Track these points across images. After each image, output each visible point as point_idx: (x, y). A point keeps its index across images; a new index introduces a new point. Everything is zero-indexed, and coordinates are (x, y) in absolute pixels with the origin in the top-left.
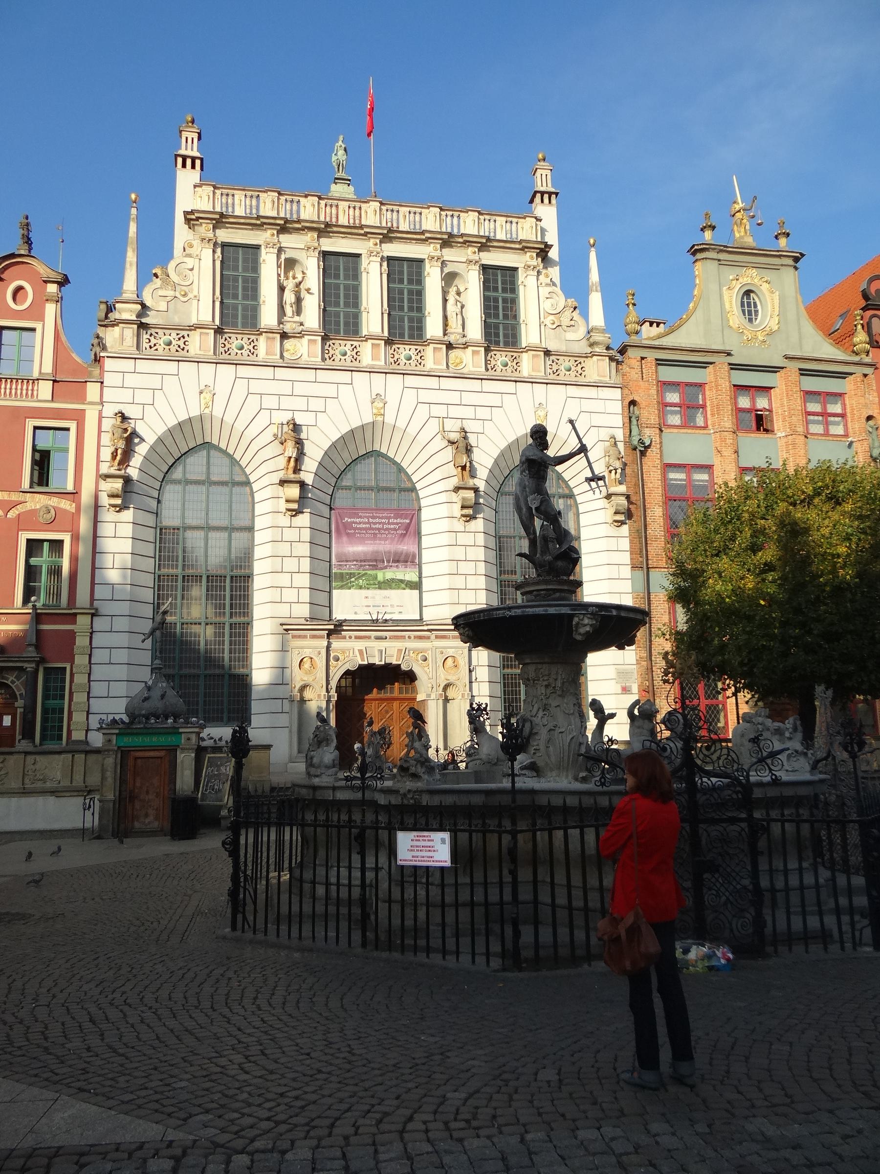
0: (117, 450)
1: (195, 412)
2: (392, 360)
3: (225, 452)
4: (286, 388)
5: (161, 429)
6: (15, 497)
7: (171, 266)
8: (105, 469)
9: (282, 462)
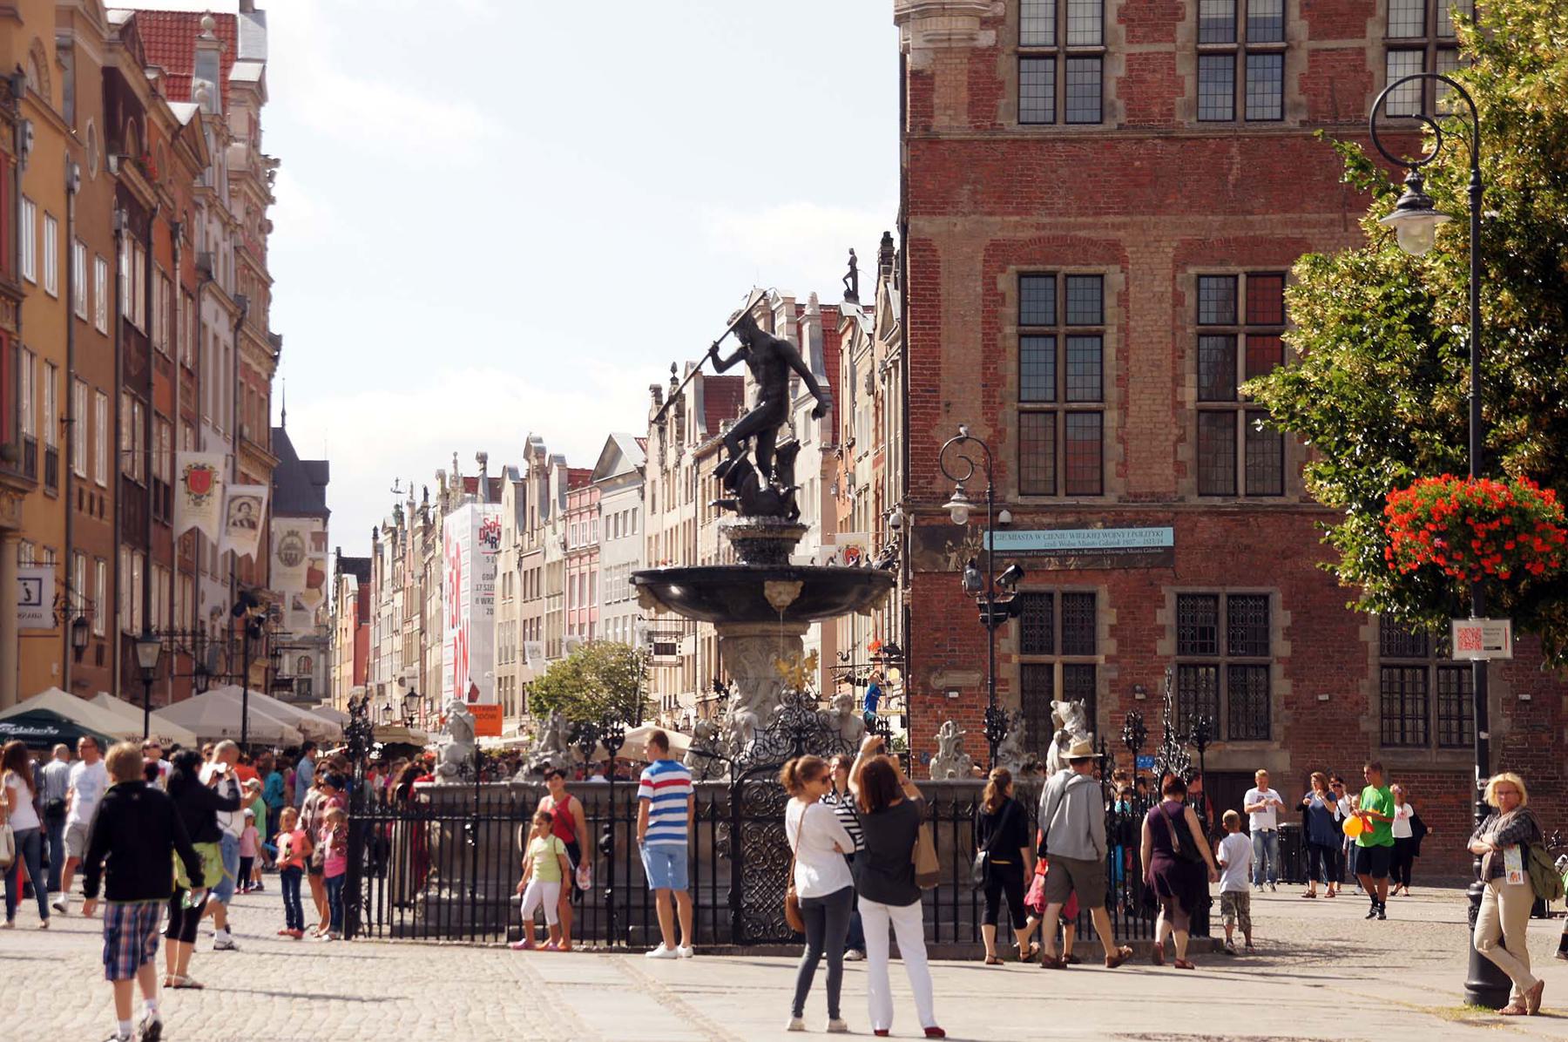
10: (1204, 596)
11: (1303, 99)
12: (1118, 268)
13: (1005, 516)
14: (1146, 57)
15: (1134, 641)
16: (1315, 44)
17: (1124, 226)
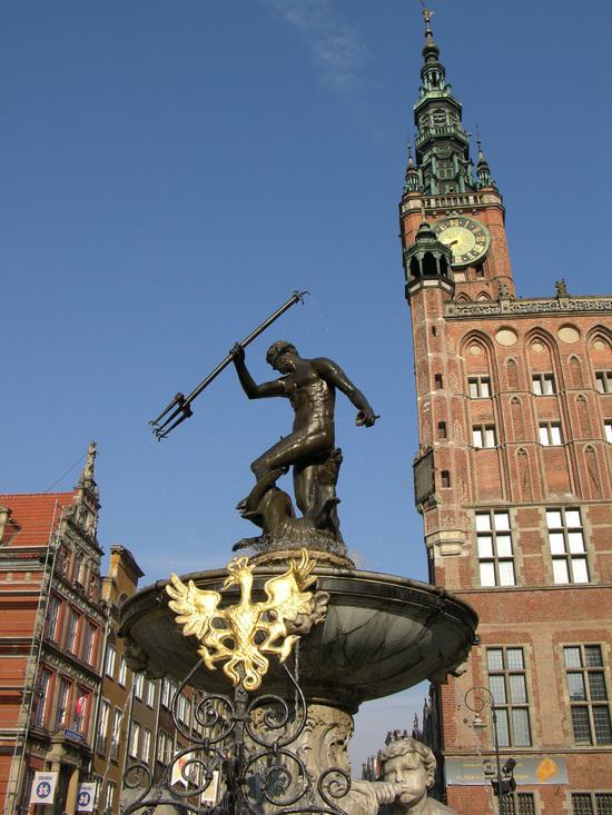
10: (584, 795)
16: (597, 553)
17: (528, 627)
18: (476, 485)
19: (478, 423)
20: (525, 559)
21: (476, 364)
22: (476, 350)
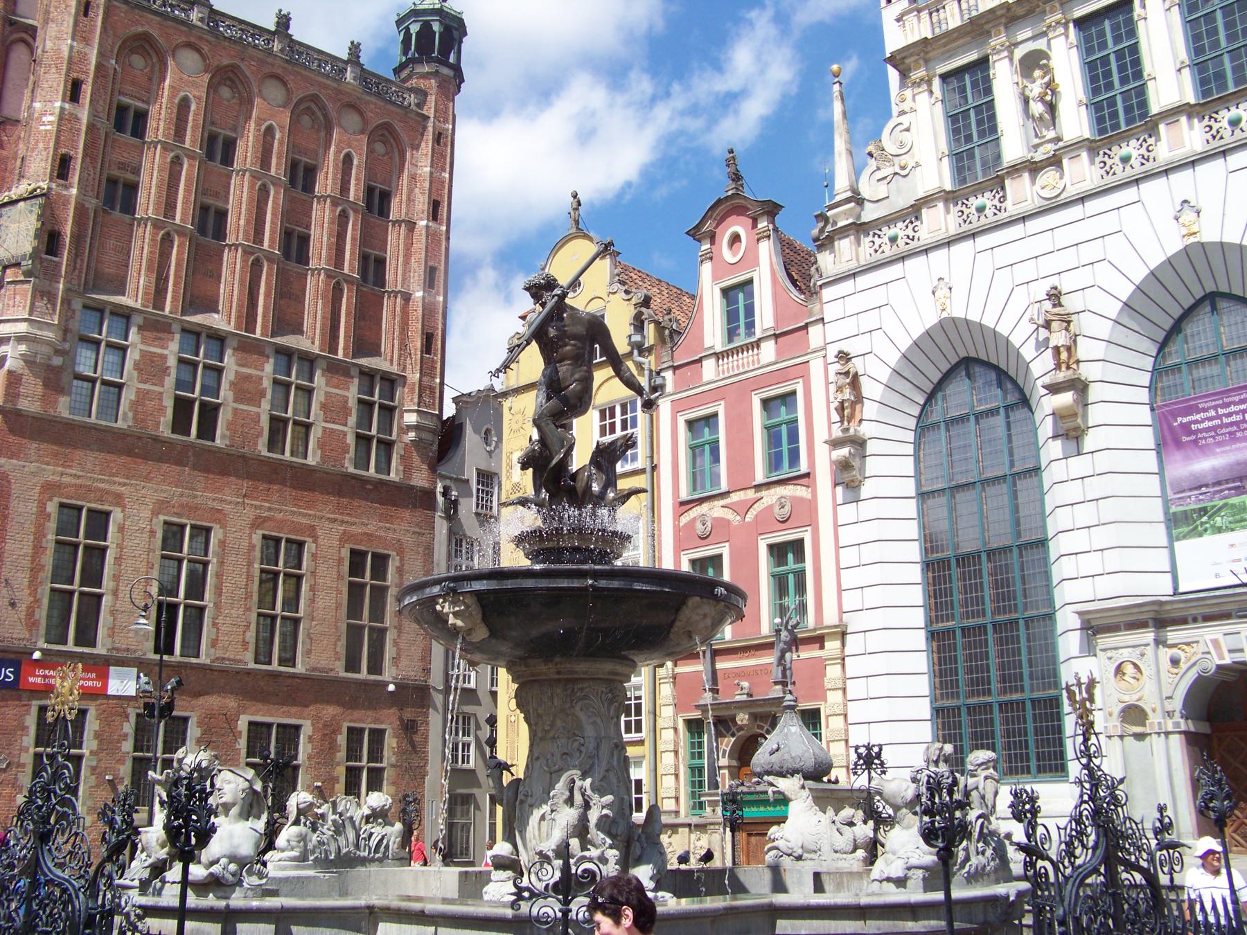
0: (842, 403)
1: (931, 320)
2: (1209, 136)
3: (987, 365)
4: (1044, 243)
5: (894, 358)
6: (751, 494)
7: (886, 131)
8: (837, 432)
9: (1048, 359)
11: (228, 433)
12: (119, 510)
13: (37, 655)
14: (148, 392)
15: (107, 742)
17: (125, 485)
18: (93, 265)
19: (116, 173)
20: (139, 391)
21: (133, 84)
22: (137, 61)
